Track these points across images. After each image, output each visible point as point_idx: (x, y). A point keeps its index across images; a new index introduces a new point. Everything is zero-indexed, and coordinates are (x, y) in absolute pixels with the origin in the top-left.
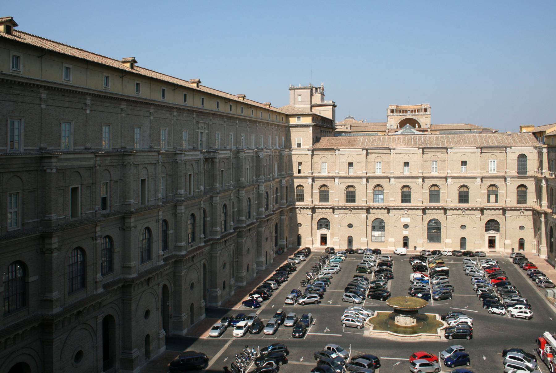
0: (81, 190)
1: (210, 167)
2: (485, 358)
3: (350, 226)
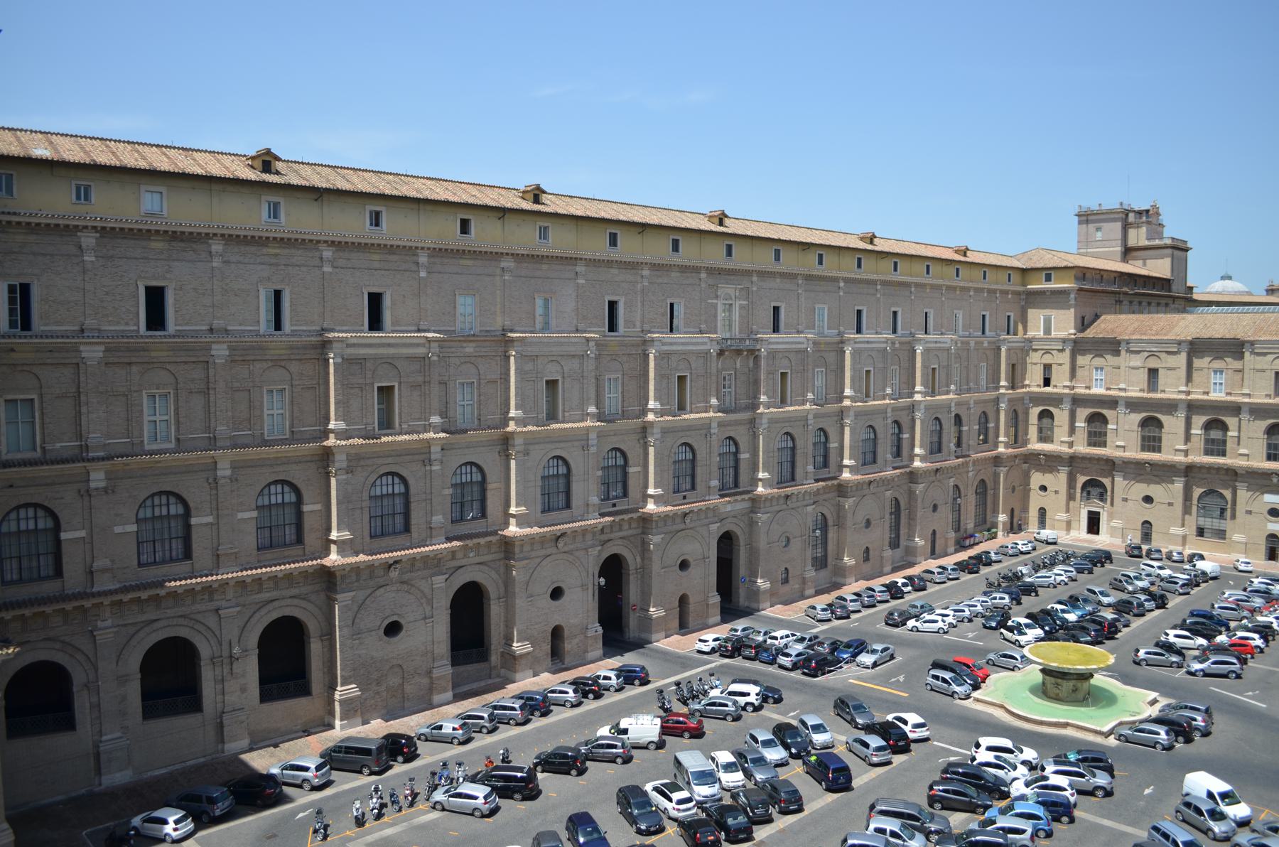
0: (400, 389)
1: (751, 364)
2: (1147, 791)
3: (1148, 499)
